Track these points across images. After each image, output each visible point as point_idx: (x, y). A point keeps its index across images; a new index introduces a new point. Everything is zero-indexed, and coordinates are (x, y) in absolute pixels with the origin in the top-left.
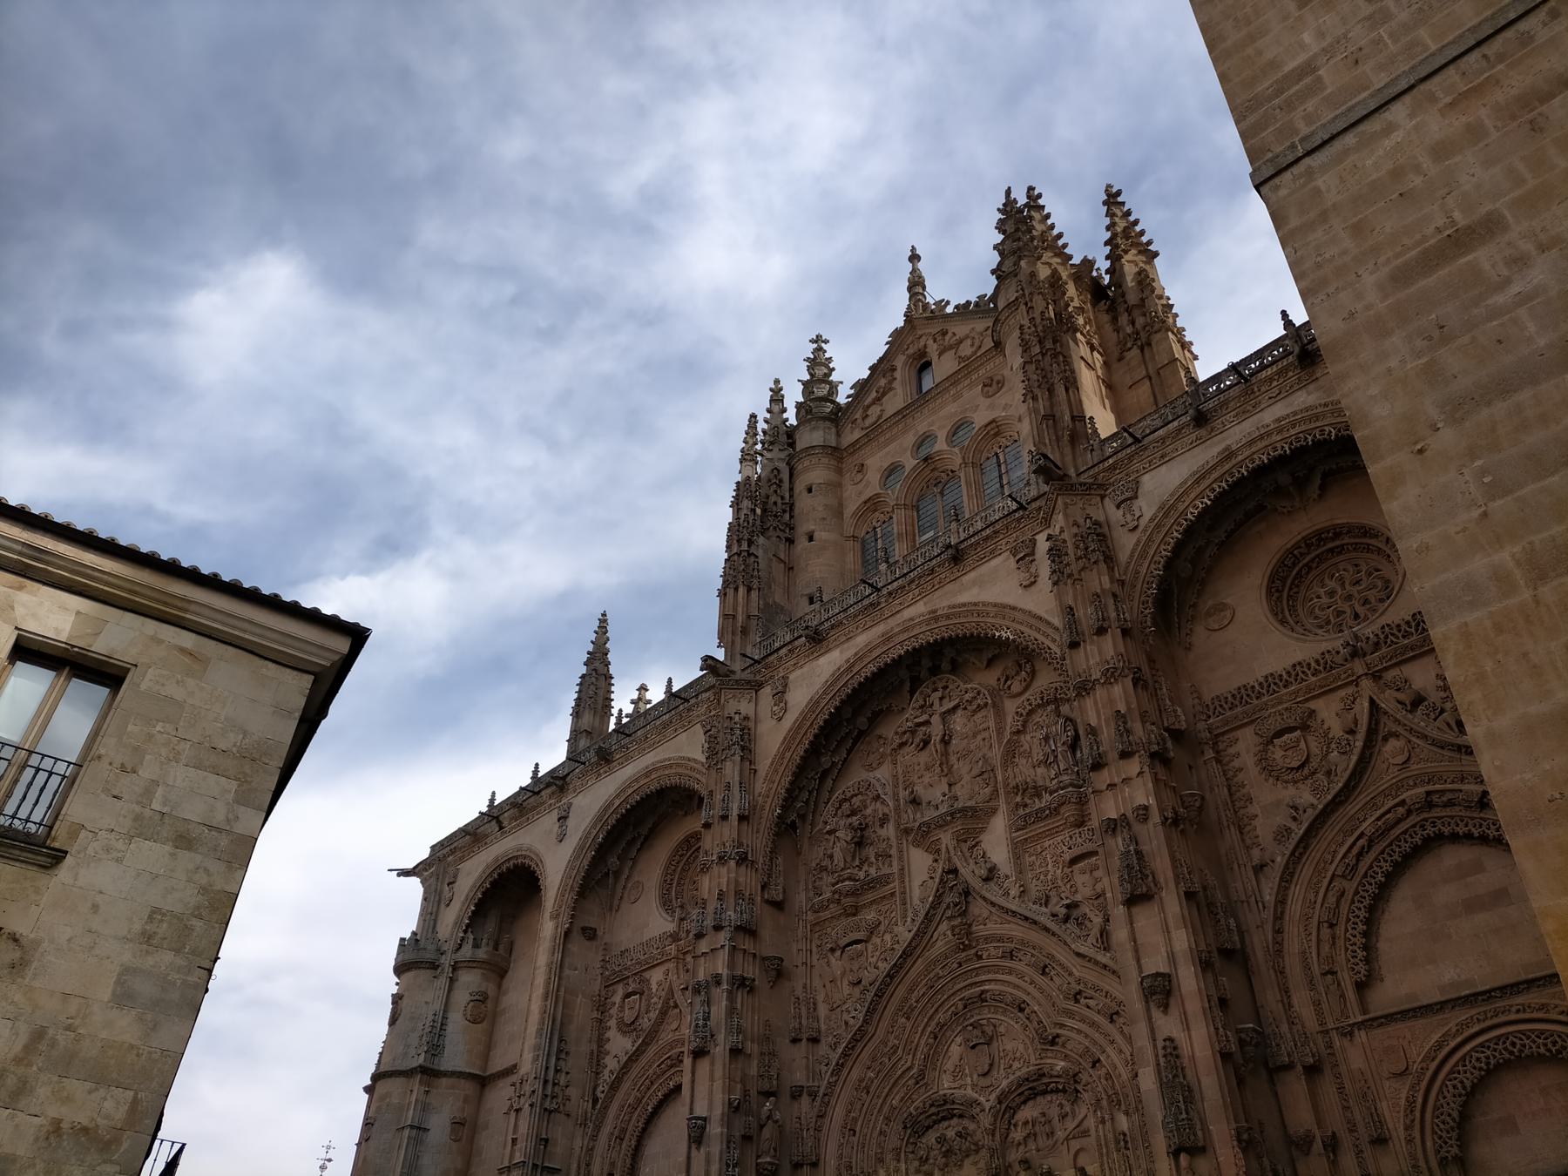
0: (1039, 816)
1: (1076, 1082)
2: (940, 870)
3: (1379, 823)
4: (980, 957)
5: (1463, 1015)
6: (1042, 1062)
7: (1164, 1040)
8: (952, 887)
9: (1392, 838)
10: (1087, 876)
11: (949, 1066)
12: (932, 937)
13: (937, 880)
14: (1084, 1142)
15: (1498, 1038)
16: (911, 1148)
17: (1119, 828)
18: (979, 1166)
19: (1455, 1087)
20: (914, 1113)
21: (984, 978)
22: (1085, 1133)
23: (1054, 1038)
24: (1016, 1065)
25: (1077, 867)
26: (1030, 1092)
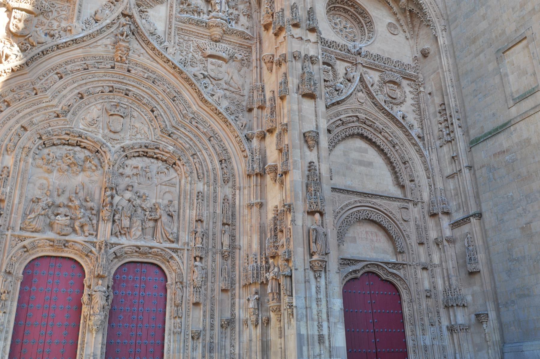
0: (198, 23)
1: (179, 160)
2: (120, 10)
3: (348, 119)
4: (129, 71)
5: (357, 198)
6: (158, 141)
7: (310, 163)
8: (127, 24)
9: (349, 126)
10: (213, 67)
11: (89, 118)
12: (96, 42)
13: (117, 14)
14: (172, 189)
15: (364, 210)
16: (37, 152)
17: (301, 60)
18: (92, 178)
19: (347, 221)
20: (52, 133)
21: (129, 82)
22: (173, 185)
23: (172, 133)
24: (139, 136)
25: (210, 60)
26: (143, 153)
